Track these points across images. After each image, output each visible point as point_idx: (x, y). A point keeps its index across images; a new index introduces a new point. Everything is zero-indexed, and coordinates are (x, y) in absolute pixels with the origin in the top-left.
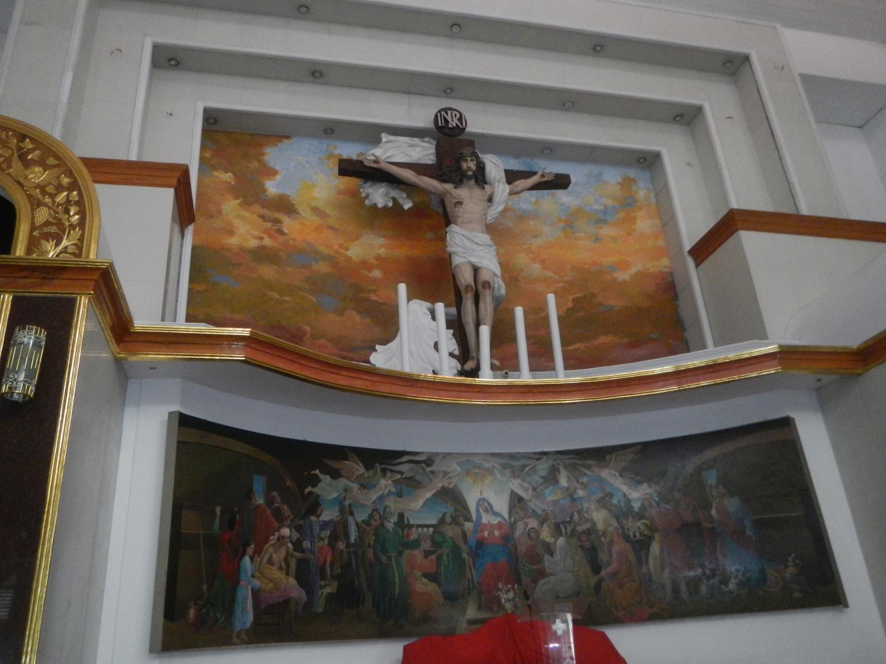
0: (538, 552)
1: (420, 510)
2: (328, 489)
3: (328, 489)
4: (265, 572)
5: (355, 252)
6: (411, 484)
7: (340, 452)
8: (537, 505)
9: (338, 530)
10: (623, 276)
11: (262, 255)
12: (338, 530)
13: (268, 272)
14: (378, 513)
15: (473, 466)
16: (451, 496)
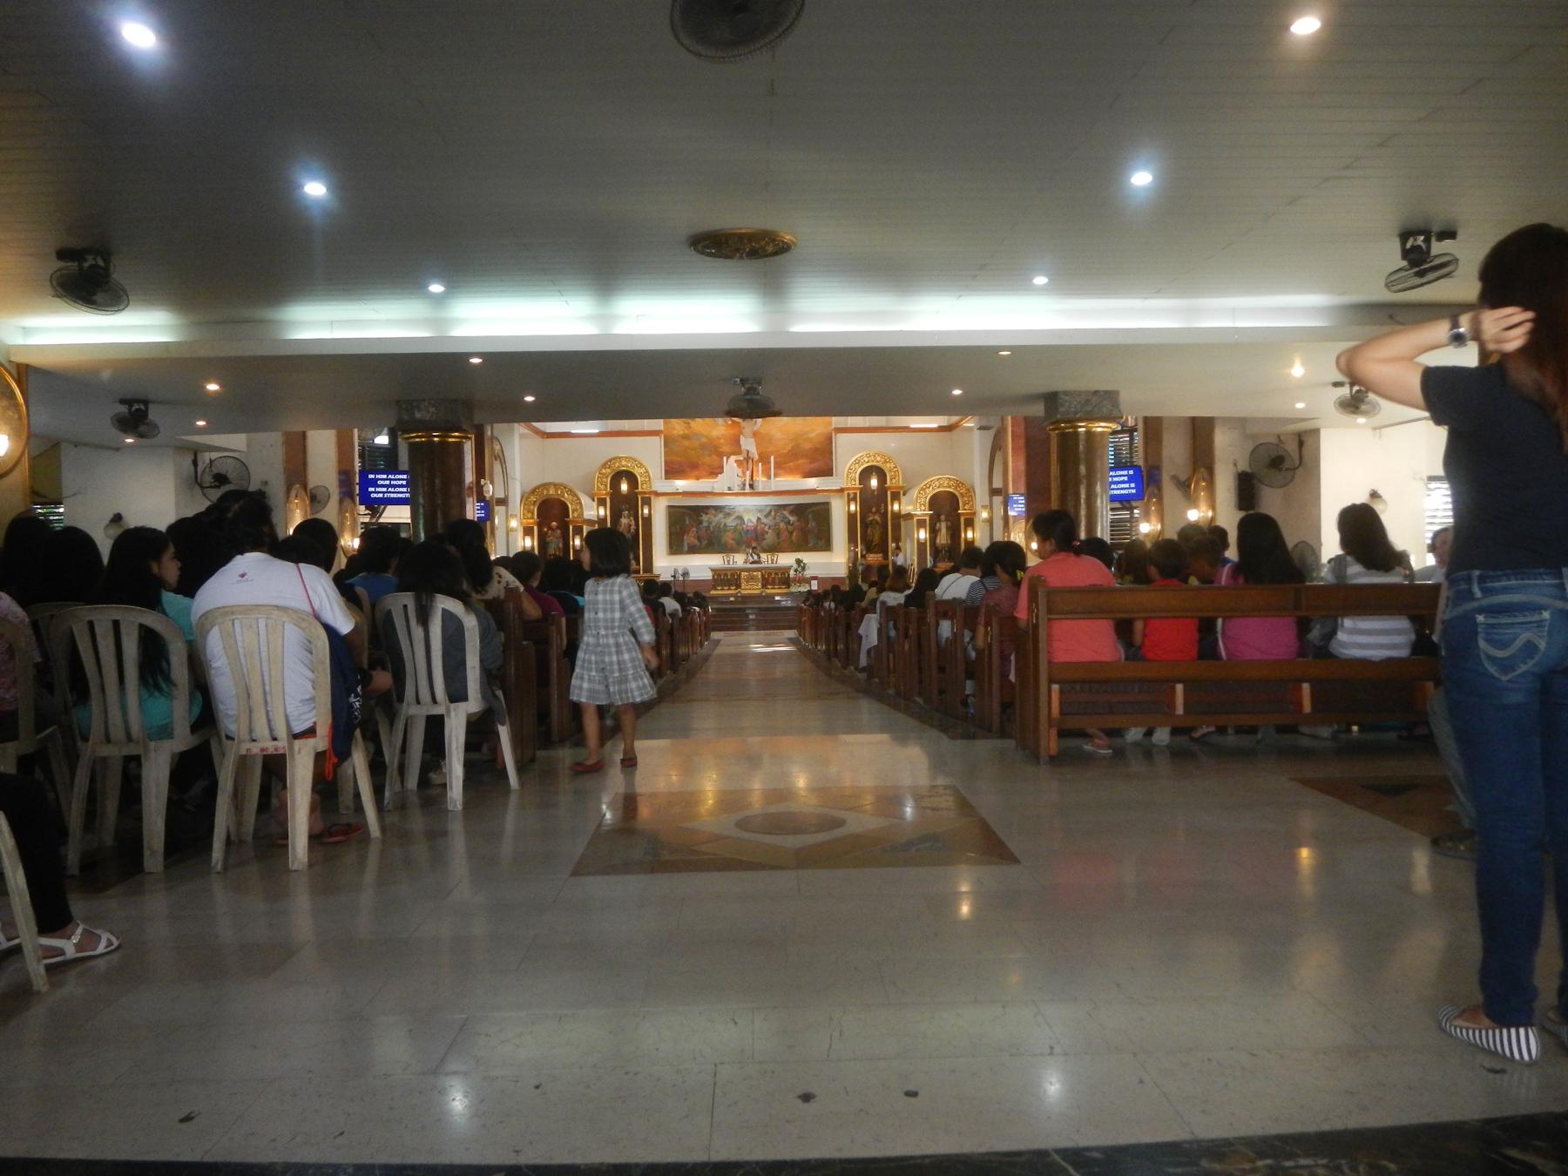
0: (764, 533)
1: (731, 522)
2: (705, 518)
3: (705, 518)
4: (689, 539)
5: (715, 433)
6: (729, 515)
7: (707, 507)
8: (764, 520)
9: (708, 528)
10: (812, 435)
11: (685, 437)
12: (708, 528)
13: (686, 443)
14: (718, 524)
15: (748, 511)
16: (740, 518)
